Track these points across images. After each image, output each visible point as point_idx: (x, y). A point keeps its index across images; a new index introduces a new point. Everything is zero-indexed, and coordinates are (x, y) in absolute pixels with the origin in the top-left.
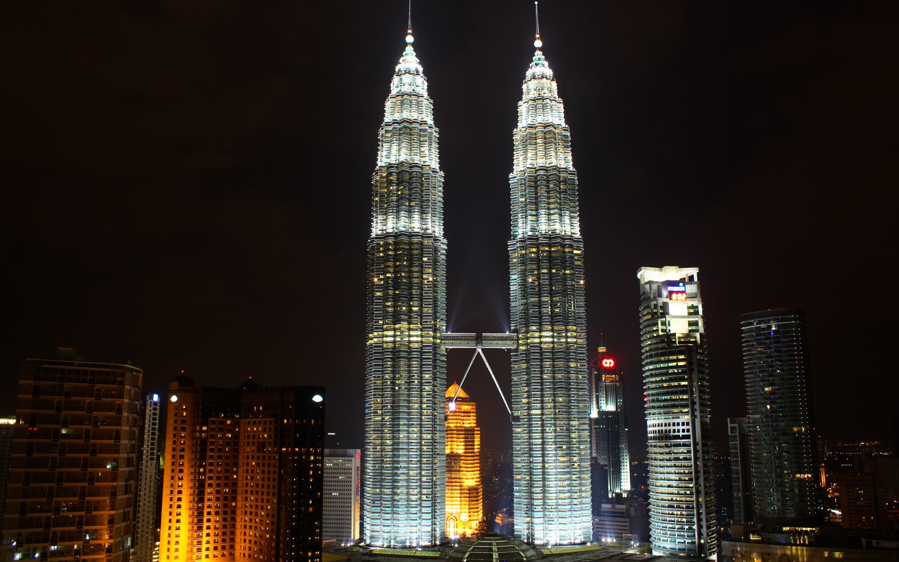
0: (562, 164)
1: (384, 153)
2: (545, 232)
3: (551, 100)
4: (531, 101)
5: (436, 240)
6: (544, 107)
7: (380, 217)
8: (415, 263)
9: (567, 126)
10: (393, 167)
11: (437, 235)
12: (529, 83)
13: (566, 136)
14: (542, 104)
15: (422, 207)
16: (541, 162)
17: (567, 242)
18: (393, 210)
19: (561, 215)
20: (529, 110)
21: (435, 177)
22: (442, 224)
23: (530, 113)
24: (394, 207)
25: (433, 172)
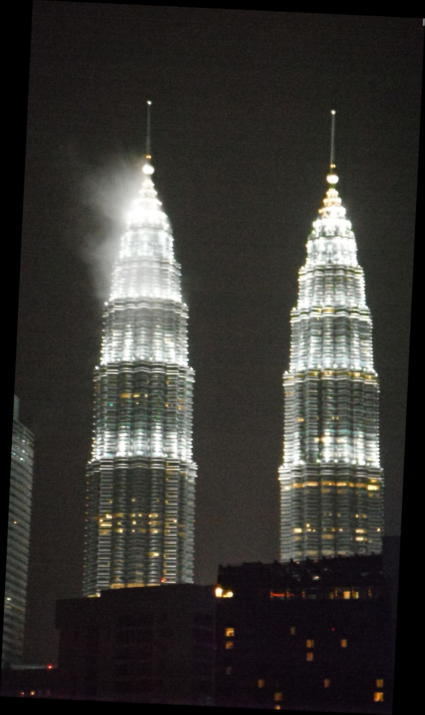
0: (357, 365)
1: (114, 344)
2: (329, 460)
3: (345, 271)
4: (318, 272)
5: (183, 466)
6: (335, 280)
7: (107, 435)
8: (155, 500)
9: (367, 308)
10: (126, 366)
11: (183, 459)
12: (317, 242)
13: (365, 323)
14: (333, 276)
15: (165, 422)
16: (328, 362)
17: (360, 475)
18: (126, 425)
19: (352, 437)
20: (313, 284)
21: (184, 379)
22: (191, 443)
23: (316, 289)
24: (128, 421)
25: (181, 371)
